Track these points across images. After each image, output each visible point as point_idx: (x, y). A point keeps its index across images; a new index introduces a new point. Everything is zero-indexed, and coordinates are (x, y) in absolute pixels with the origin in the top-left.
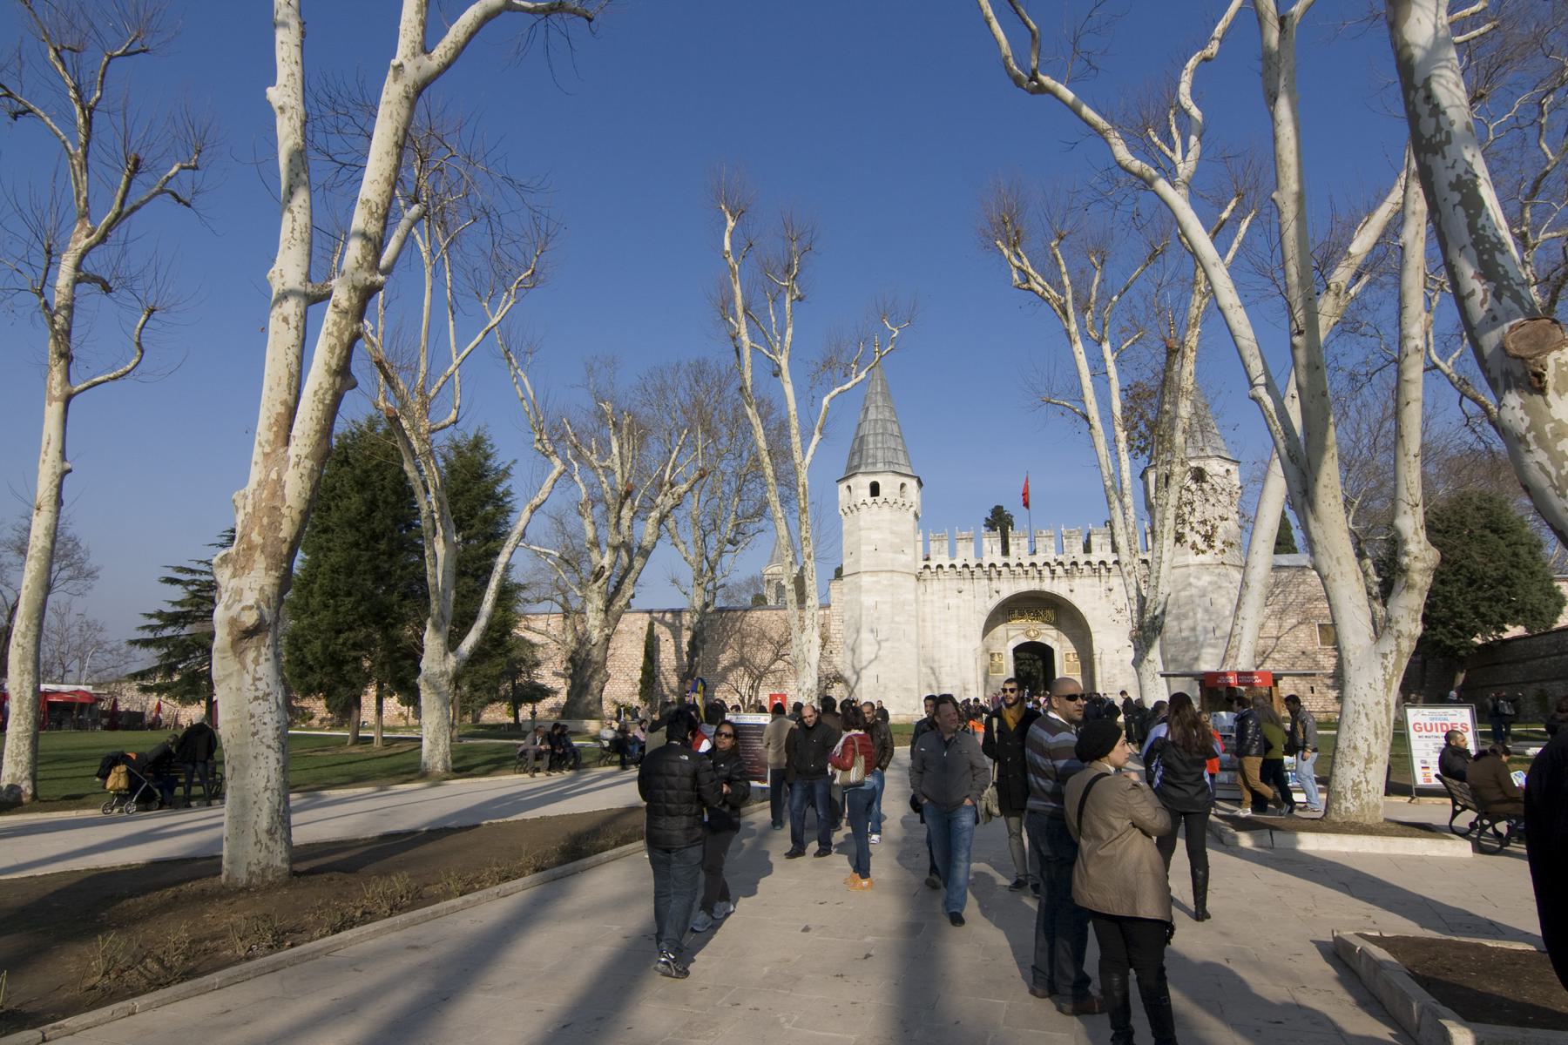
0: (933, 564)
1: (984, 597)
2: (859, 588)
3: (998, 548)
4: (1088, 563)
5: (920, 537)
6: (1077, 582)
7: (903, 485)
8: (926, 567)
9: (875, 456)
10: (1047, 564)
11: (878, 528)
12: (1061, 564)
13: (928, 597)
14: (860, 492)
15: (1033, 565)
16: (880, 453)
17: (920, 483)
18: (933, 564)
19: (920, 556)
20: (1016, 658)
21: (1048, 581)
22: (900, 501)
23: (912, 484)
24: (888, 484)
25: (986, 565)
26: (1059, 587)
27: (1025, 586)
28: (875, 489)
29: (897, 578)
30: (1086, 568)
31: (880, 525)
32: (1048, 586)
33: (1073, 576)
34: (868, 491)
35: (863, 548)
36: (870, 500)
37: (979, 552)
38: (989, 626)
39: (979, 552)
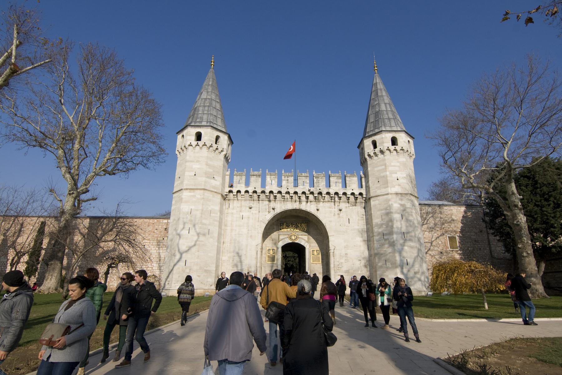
0: (235, 190)
1: (265, 213)
2: (181, 199)
3: (275, 182)
4: (328, 193)
5: (228, 173)
6: (321, 205)
7: (217, 138)
8: (230, 192)
9: (202, 118)
10: (304, 193)
11: (198, 161)
12: (312, 193)
13: (230, 211)
14: (188, 137)
15: (296, 193)
16: (205, 117)
17: (230, 137)
18: (235, 190)
19: (227, 184)
20: (284, 257)
21: (304, 203)
22: (215, 146)
23: (224, 139)
24: (208, 135)
25: (267, 191)
26: (310, 207)
27: (290, 206)
28: (199, 137)
29: (207, 194)
30: (327, 196)
31: (199, 159)
32: (304, 206)
33: (319, 201)
34: (194, 138)
35: (187, 174)
36: (194, 143)
37: (263, 184)
38: (267, 233)
39: (263, 184)
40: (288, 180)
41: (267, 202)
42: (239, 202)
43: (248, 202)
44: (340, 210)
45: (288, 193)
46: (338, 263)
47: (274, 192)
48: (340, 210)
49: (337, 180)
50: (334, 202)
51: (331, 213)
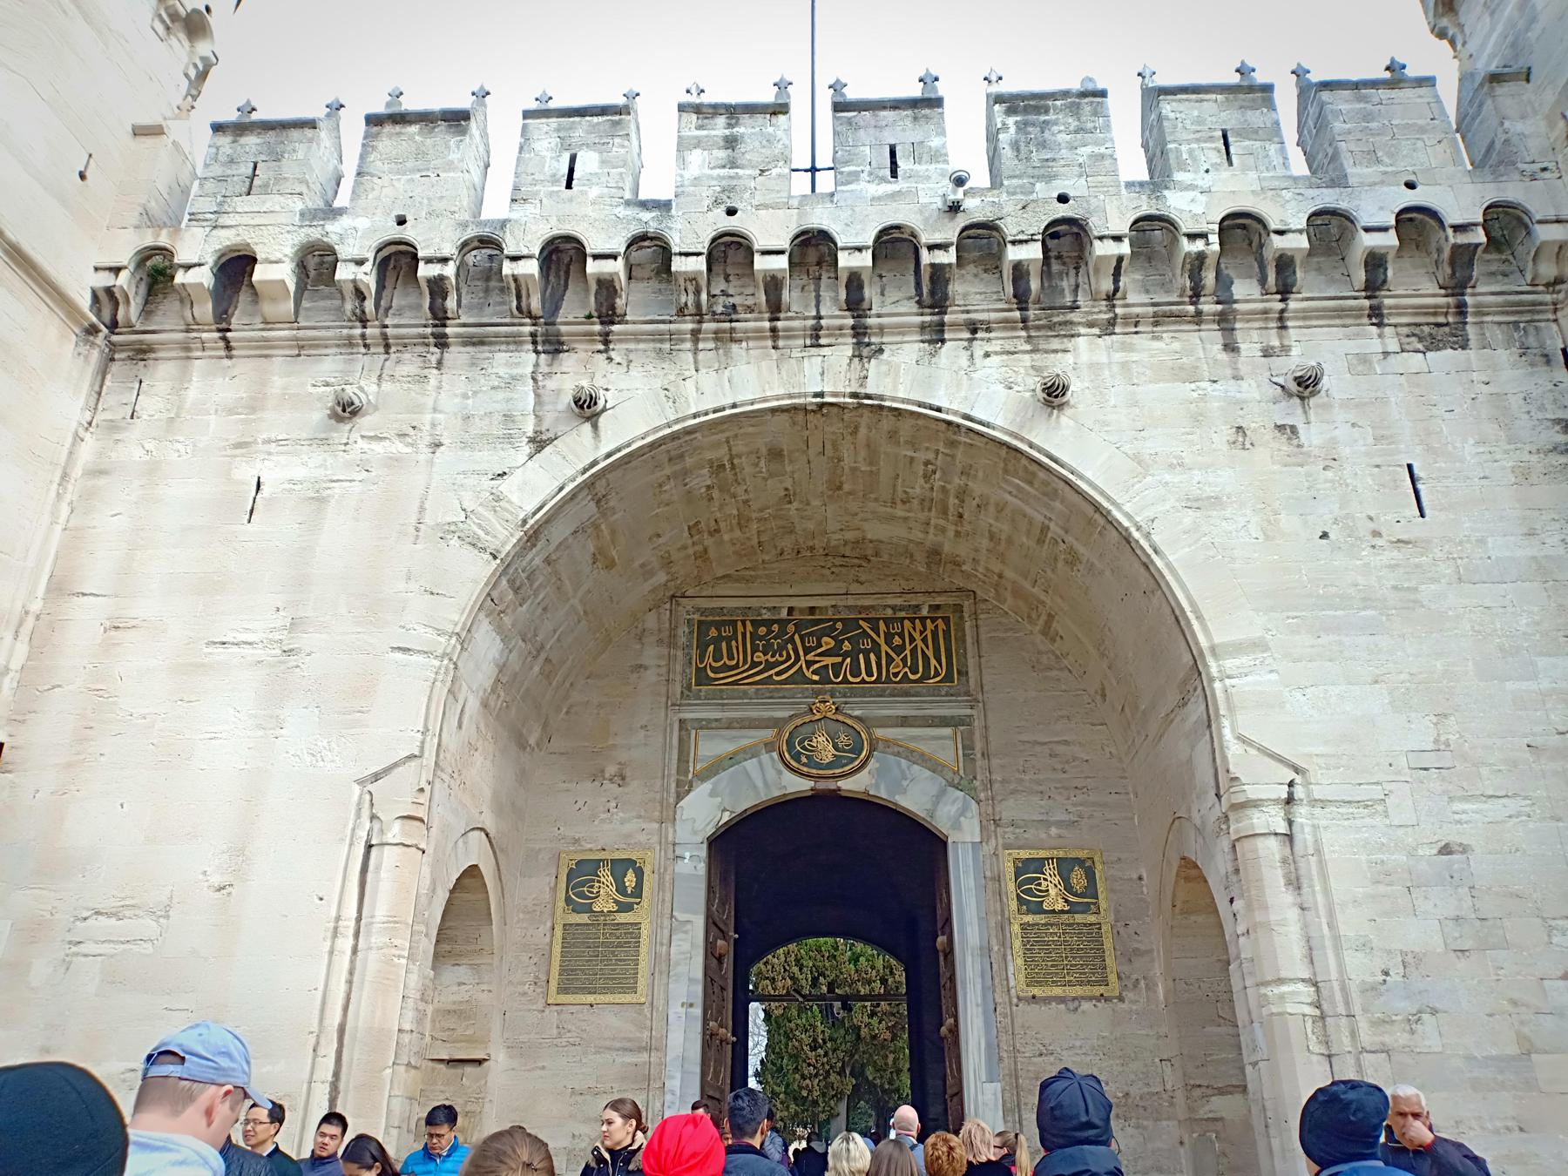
6: (1083, 357)
13: (132, 449)
27: (752, 378)
32: (908, 375)
40: (731, 142)
41: (527, 359)
42: (243, 367)
43: (329, 366)
44: (1307, 385)
45: (729, 251)
46: (1360, 968)
47: (593, 244)
48: (1307, 385)
49: (1230, 118)
50: (1225, 321)
51: (1197, 419)
